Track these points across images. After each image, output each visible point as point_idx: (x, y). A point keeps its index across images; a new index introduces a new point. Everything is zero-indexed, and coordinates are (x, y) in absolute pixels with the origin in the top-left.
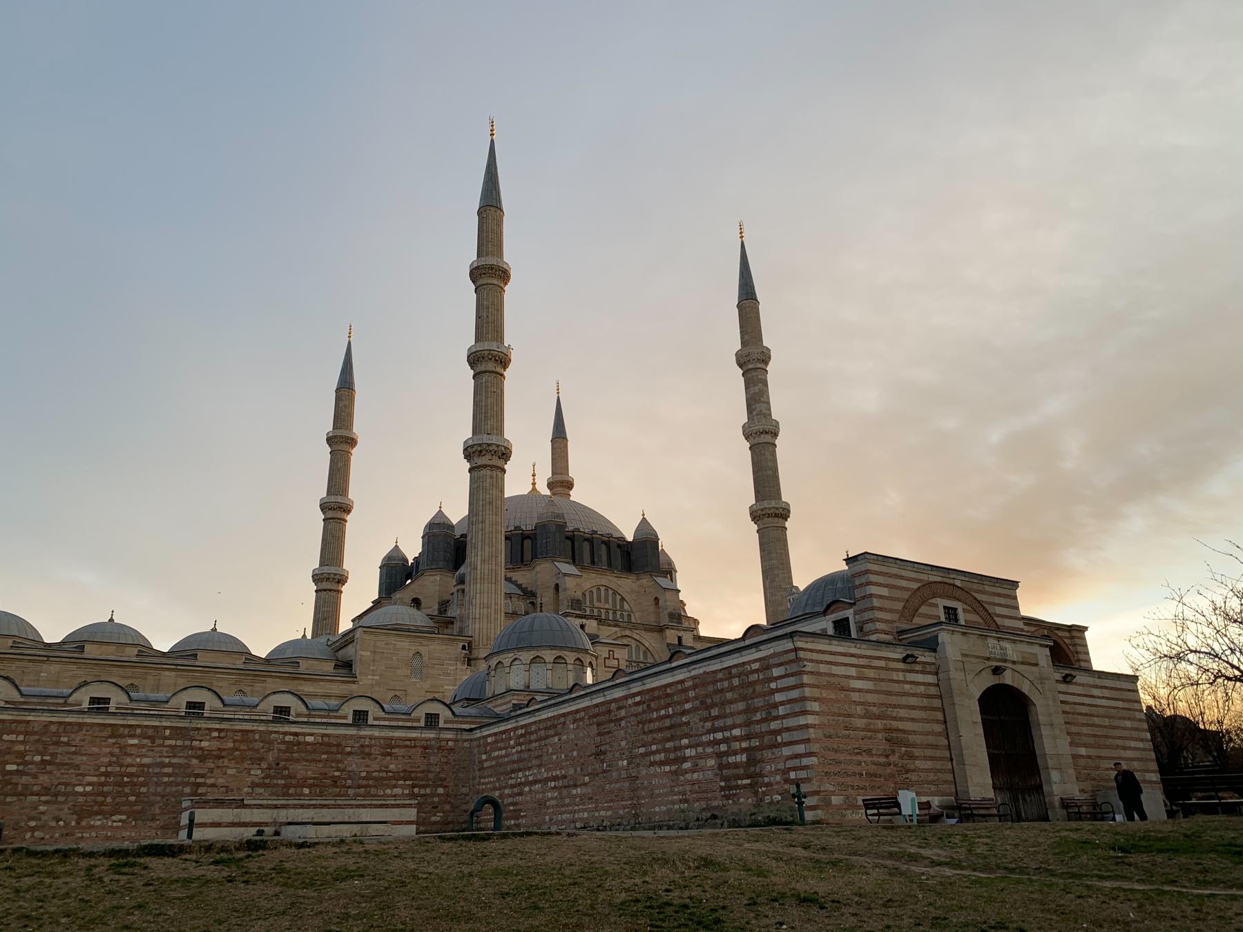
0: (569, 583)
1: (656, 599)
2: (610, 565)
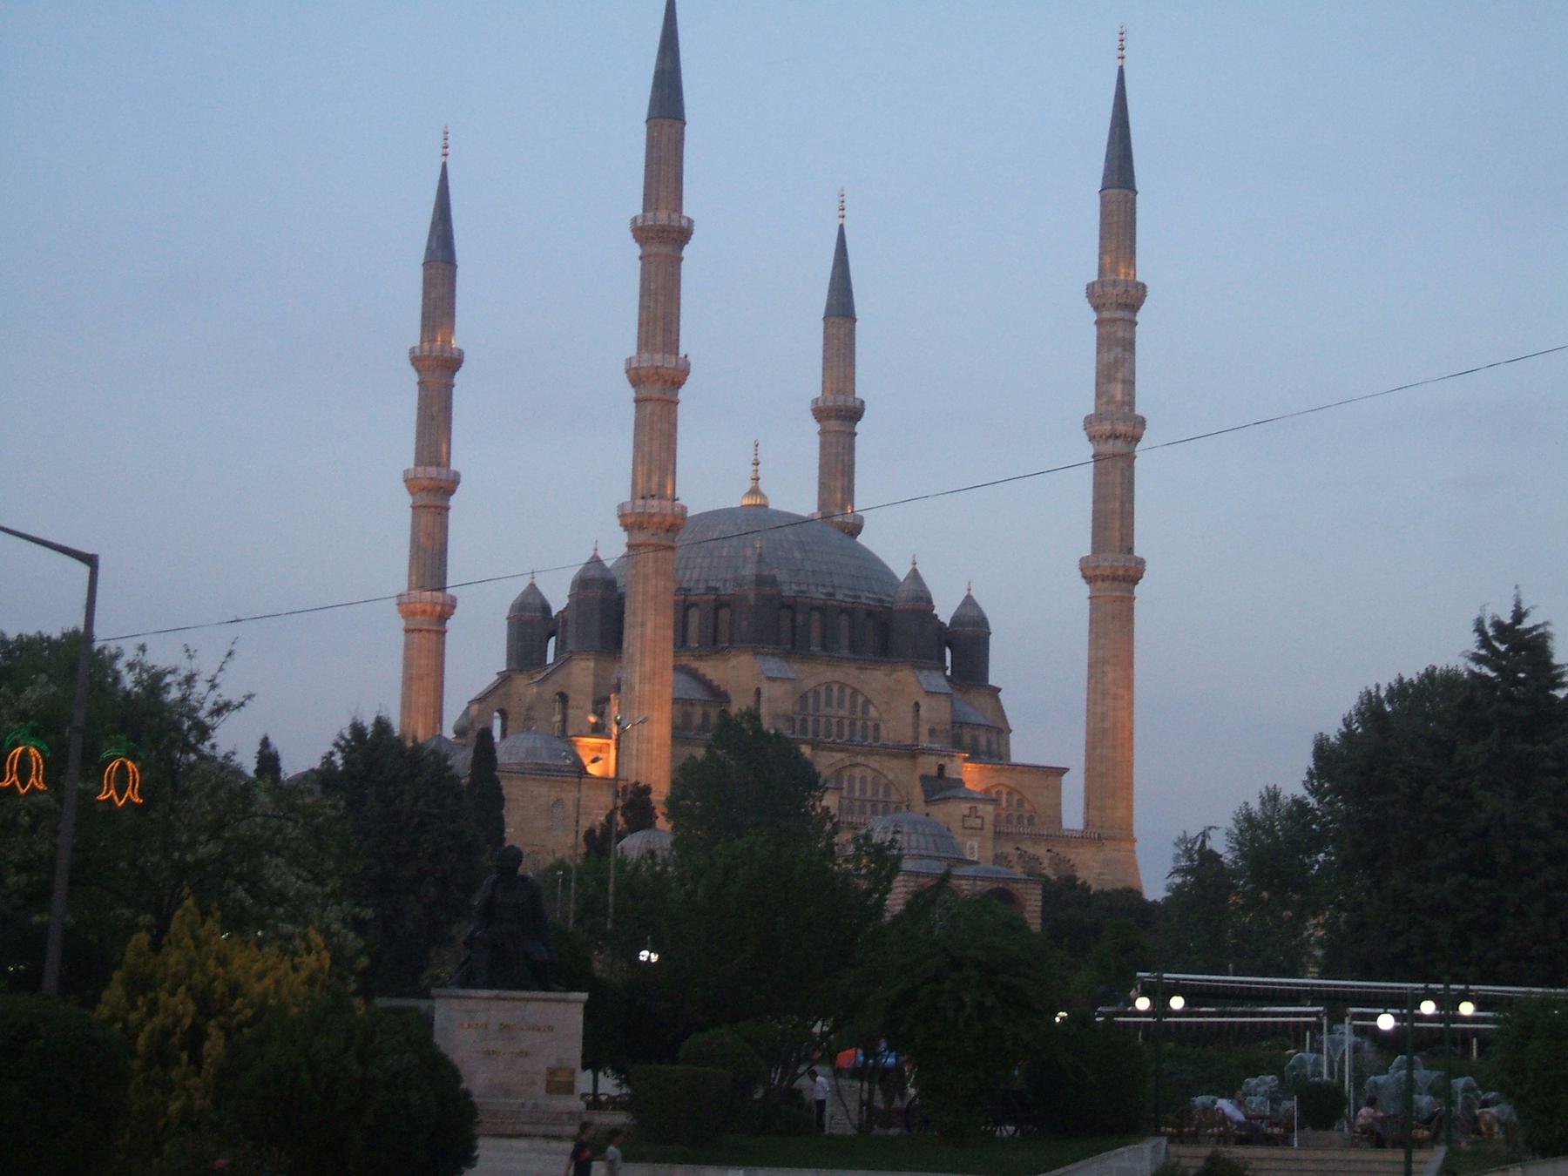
1: (917, 705)
2: (853, 648)
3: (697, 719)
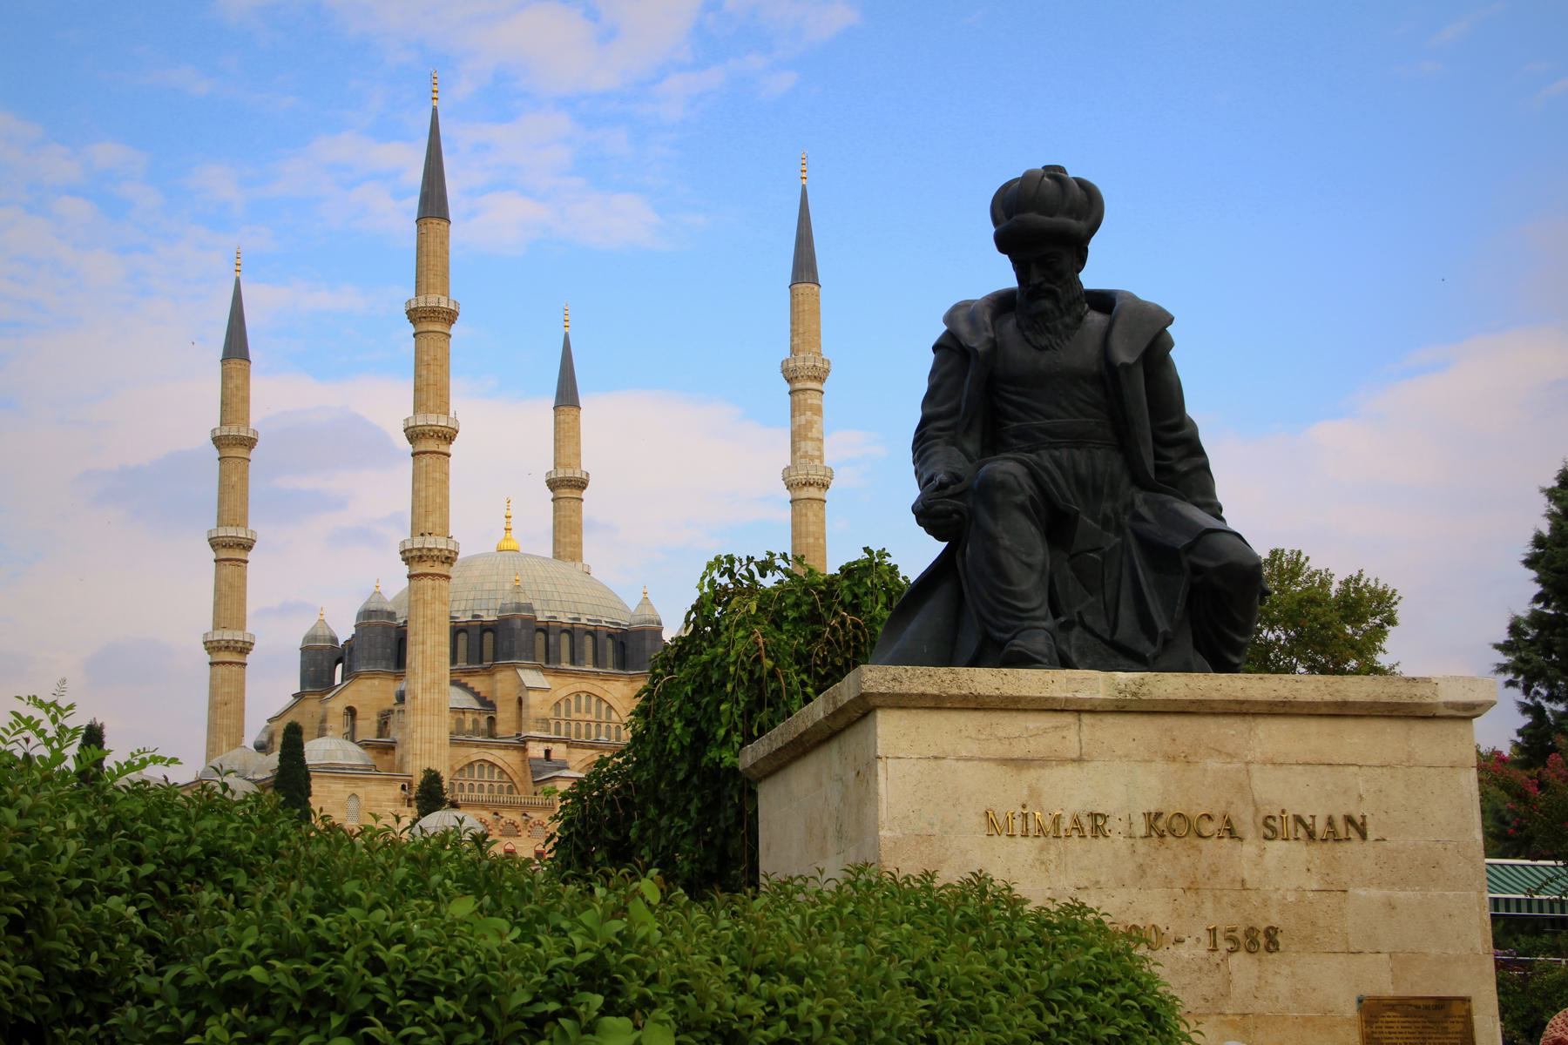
0: (533, 698)
3: (469, 725)
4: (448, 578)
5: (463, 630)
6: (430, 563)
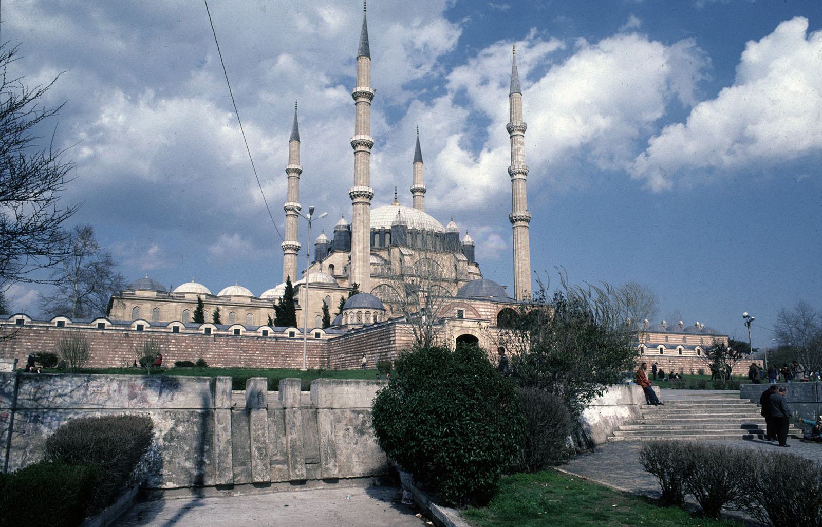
0: (407, 259)
4: (370, 204)
5: (376, 233)
6: (361, 197)
